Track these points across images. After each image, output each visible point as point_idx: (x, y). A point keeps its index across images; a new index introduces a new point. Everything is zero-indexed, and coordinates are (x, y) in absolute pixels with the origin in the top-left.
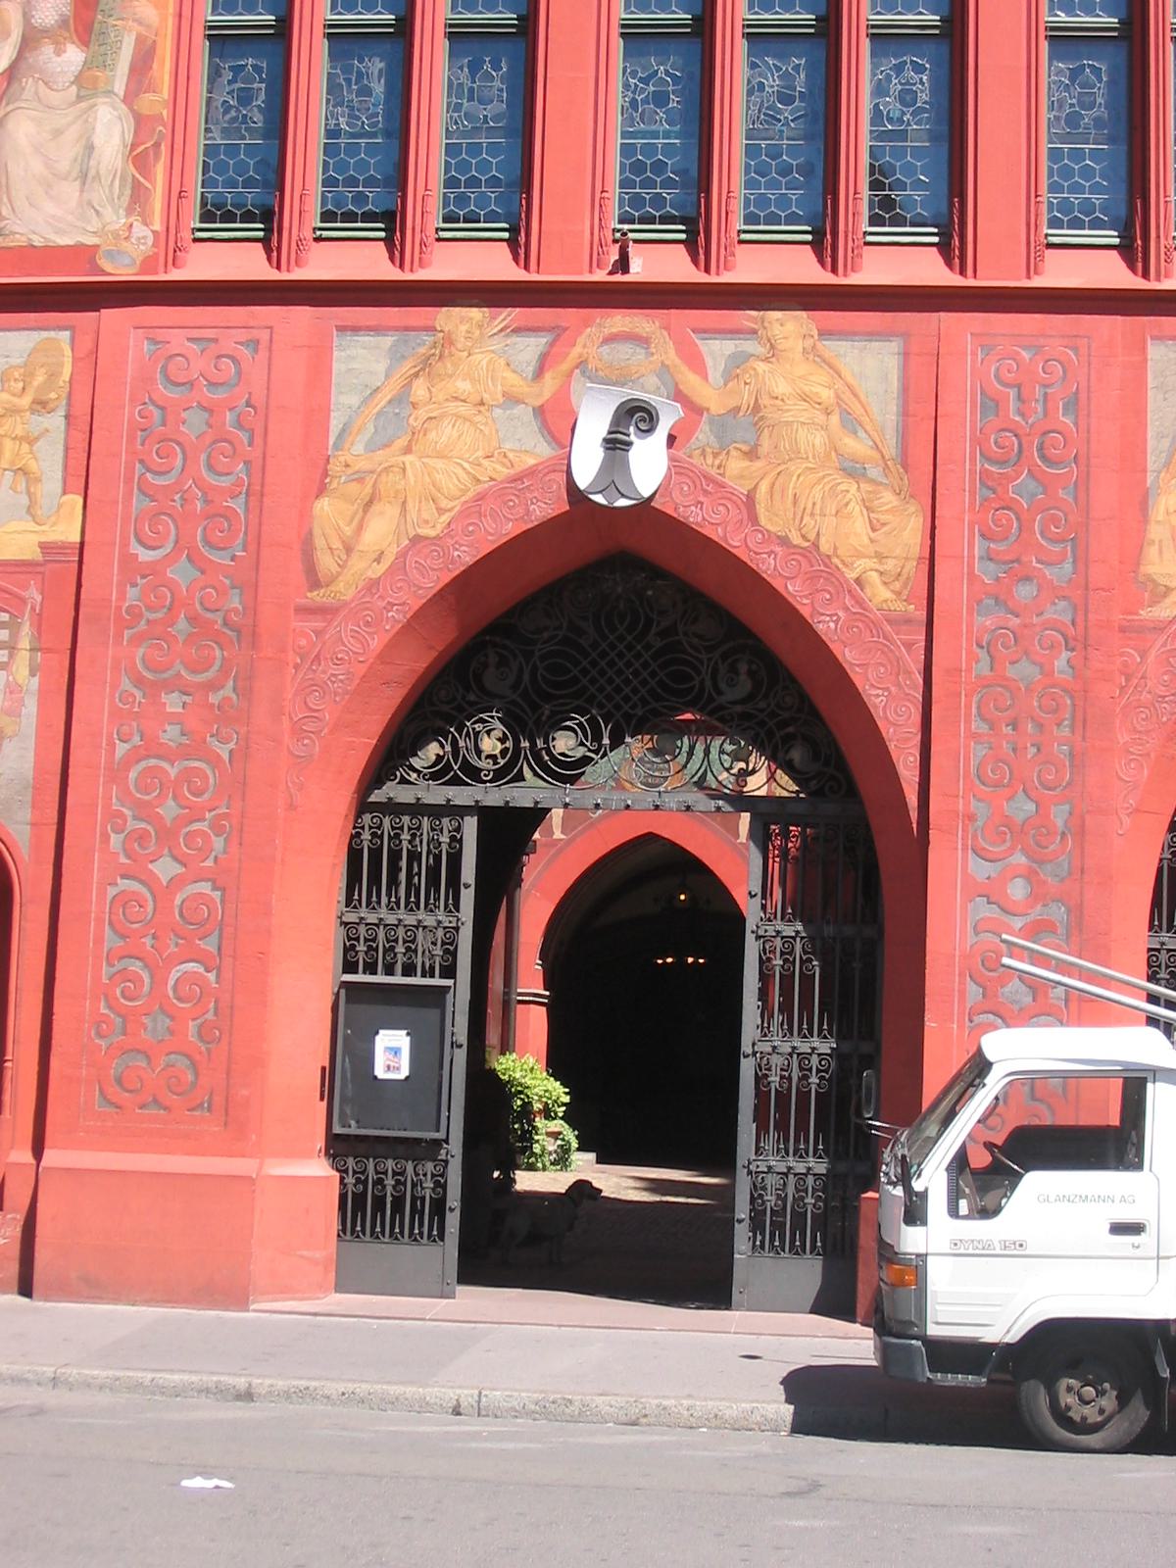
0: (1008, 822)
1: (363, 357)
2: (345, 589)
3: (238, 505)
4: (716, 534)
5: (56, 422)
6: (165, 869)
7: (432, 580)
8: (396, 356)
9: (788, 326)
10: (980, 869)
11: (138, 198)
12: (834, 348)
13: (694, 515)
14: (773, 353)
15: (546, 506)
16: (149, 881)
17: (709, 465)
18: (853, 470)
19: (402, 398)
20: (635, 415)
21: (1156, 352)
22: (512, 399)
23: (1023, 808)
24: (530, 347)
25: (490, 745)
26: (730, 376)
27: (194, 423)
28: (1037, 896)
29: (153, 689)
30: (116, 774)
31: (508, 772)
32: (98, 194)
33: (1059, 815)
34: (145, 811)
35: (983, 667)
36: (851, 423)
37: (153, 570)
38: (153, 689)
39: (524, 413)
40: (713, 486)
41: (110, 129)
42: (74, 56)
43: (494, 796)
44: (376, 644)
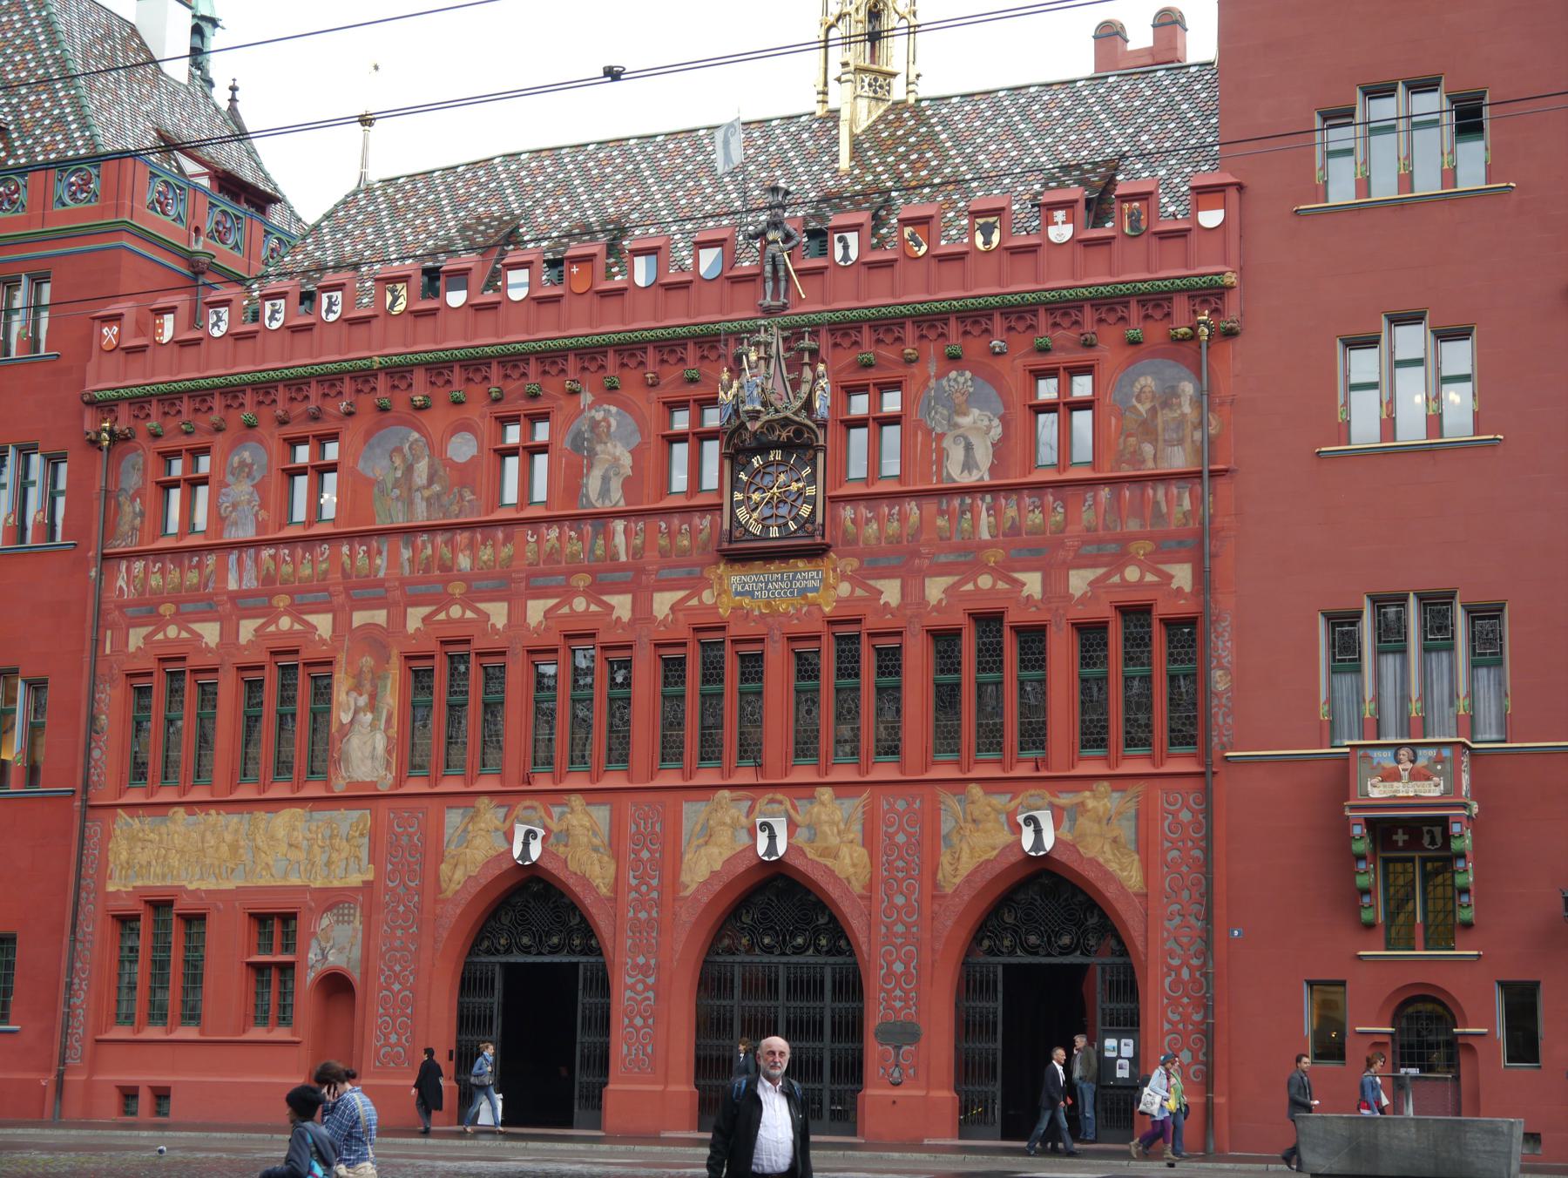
0: (637, 965)
1: (454, 818)
2: (449, 894)
3: (417, 867)
4: (555, 872)
5: (366, 840)
6: (396, 987)
7: (474, 890)
8: (464, 816)
9: (577, 801)
10: (630, 981)
11: (388, 766)
12: (591, 809)
13: (550, 865)
14: (573, 811)
15: (505, 866)
16: (391, 991)
17: (554, 849)
18: (596, 849)
19: (465, 830)
20: (530, 834)
21: (685, 806)
22: (497, 829)
23: (641, 960)
24: (502, 811)
25: (503, 941)
26: (560, 819)
27: (405, 840)
28: (647, 988)
29: (393, 929)
30: (382, 956)
31: (508, 951)
32: (377, 764)
33: (653, 962)
34: (391, 968)
35: (631, 914)
36: (595, 834)
37: (393, 890)
38: (393, 929)
39: (500, 834)
40: (555, 856)
41: (380, 741)
42: (369, 716)
43: (504, 959)
44: (458, 911)
